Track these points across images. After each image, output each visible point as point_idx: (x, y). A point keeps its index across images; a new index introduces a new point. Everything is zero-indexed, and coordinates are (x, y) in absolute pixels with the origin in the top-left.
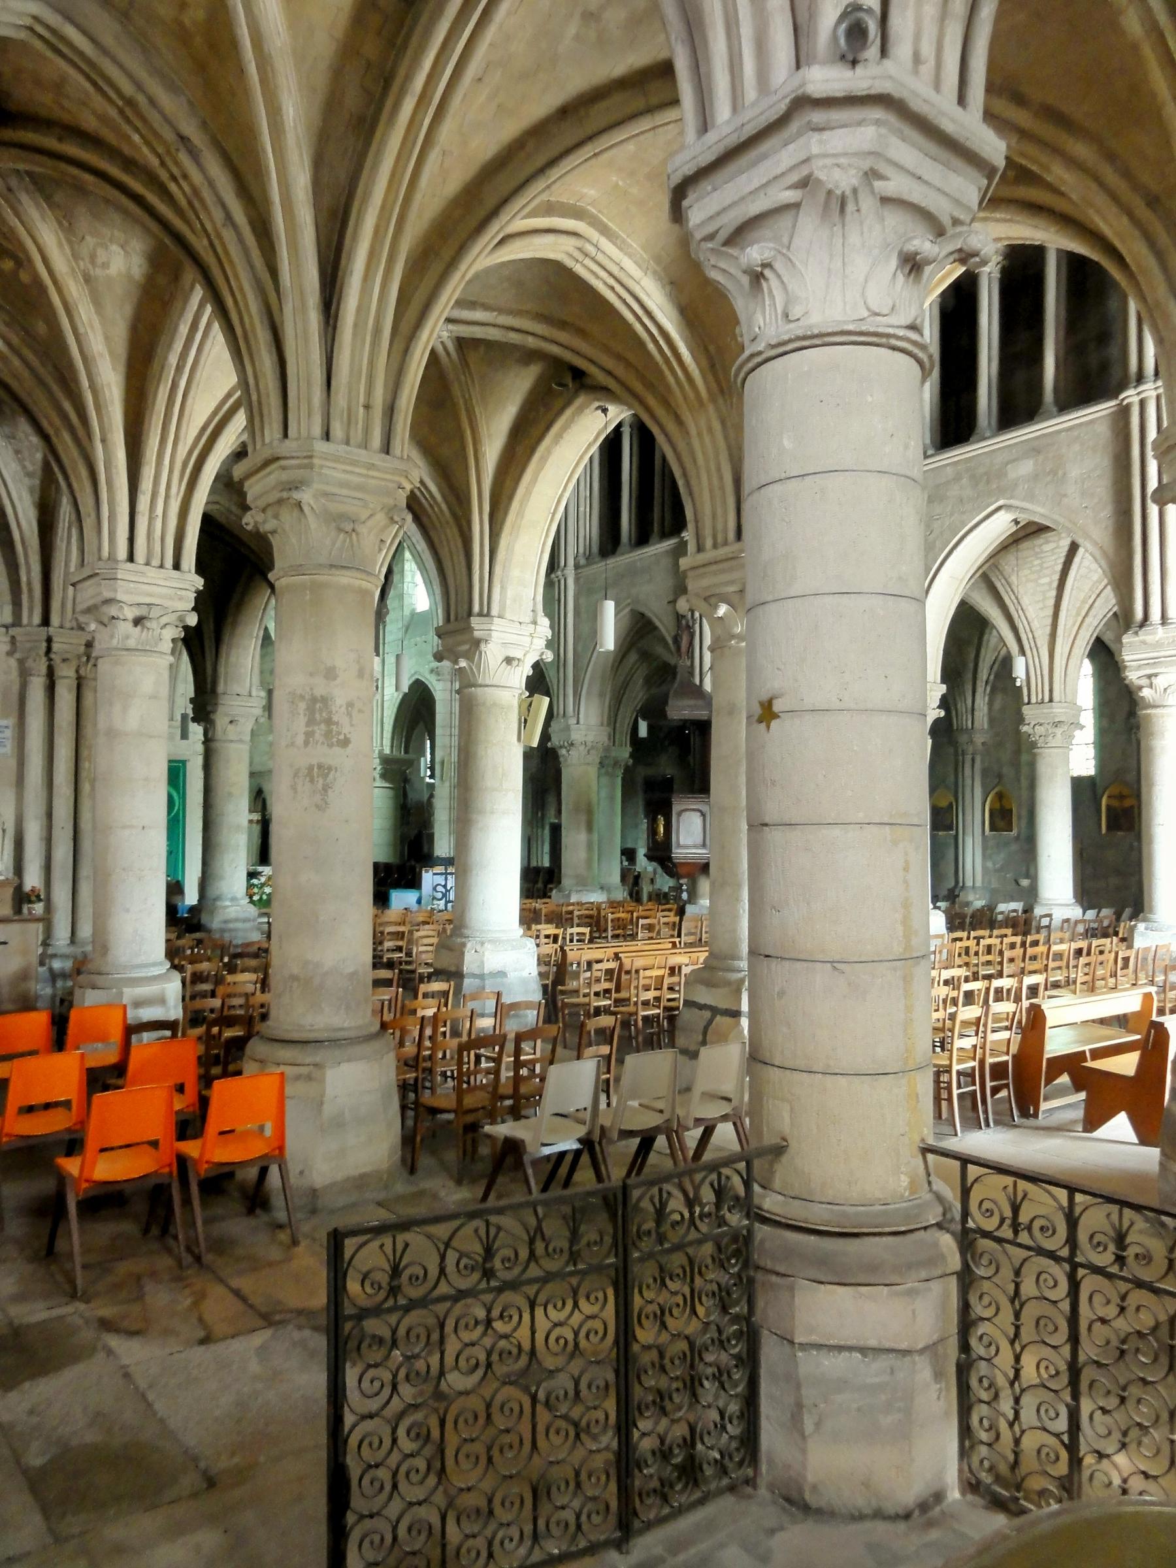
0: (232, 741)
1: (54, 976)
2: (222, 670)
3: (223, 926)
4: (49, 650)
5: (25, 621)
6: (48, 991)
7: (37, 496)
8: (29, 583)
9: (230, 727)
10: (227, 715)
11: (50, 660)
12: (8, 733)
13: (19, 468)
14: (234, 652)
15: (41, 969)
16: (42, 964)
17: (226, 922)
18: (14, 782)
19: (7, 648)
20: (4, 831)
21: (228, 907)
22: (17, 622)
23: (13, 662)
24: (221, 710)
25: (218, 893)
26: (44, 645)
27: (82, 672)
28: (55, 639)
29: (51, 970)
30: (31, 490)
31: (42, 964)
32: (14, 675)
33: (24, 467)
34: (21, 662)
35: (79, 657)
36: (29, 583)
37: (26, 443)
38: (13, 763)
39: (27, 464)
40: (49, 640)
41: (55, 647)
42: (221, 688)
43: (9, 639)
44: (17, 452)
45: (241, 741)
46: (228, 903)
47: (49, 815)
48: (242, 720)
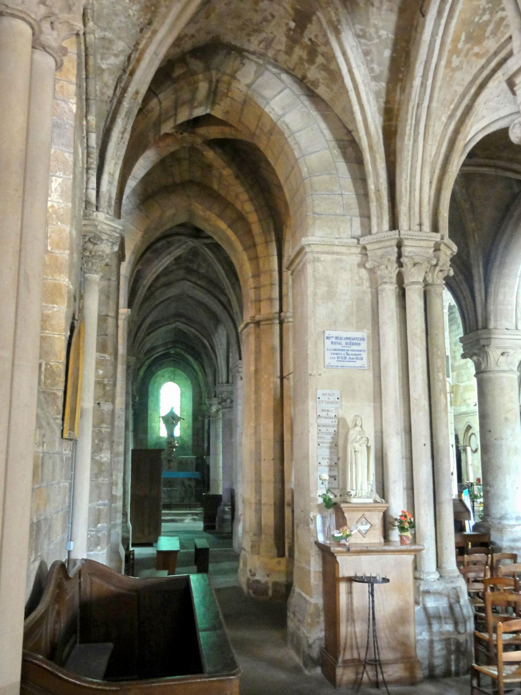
0: (504, 371)
1: (430, 618)
2: (491, 307)
3: (512, 544)
4: (400, 255)
5: (375, 229)
6: (425, 636)
7: (382, 100)
8: (378, 190)
9: (502, 359)
10: (498, 348)
11: (401, 265)
12: (364, 345)
13: (367, 72)
14: (502, 290)
15: (418, 608)
16: (417, 603)
17: (514, 540)
18: (372, 397)
19: (357, 259)
20: (368, 448)
21: (514, 526)
22: (367, 230)
23: (364, 273)
24: (493, 342)
25: (503, 512)
26: (396, 249)
27: (430, 280)
28: (406, 242)
29: (425, 609)
30: (377, 95)
31: (417, 603)
32: (367, 284)
33: (372, 70)
34: (372, 271)
35: (429, 260)
36: (378, 190)
37: (377, 40)
38: (369, 376)
39: (375, 66)
40: (399, 246)
41: (406, 251)
42: (492, 325)
43: (358, 250)
44: (366, 53)
45: (511, 371)
46: (512, 522)
47: (409, 431)
48: (511, 352)
